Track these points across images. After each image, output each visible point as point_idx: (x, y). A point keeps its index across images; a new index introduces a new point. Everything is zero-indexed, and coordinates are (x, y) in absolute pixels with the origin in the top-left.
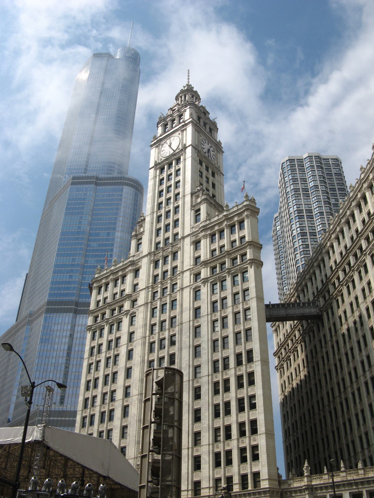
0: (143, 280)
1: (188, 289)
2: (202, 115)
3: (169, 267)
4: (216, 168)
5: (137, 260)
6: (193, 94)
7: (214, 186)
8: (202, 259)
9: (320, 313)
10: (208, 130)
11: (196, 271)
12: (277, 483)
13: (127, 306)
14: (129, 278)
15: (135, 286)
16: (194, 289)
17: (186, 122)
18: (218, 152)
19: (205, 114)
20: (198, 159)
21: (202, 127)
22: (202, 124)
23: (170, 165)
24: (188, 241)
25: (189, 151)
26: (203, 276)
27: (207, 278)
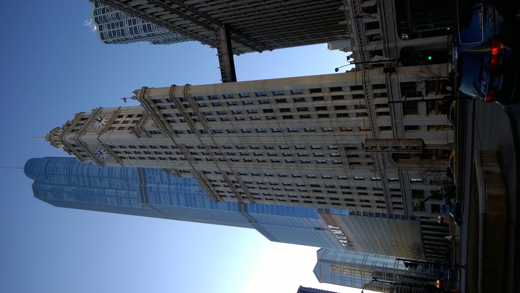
1: (214, 138)
2: (71, 128)
3: (199, 151)
4: (115, 114)
6: (52, 135)
7: (130, 116)
8: (189, 129)
9: (224, 26)
10: (83, 122)
12: (358, 72)
13: (232, 178)
14: (211, 177)
18: (101, 112)
19: (69, 125)
20: (109, 131)
21: (82, 127)
22: (78, 128)
23: (117, 152)
24: (176, 139)
25: (104, 137)
26: (203, 129)
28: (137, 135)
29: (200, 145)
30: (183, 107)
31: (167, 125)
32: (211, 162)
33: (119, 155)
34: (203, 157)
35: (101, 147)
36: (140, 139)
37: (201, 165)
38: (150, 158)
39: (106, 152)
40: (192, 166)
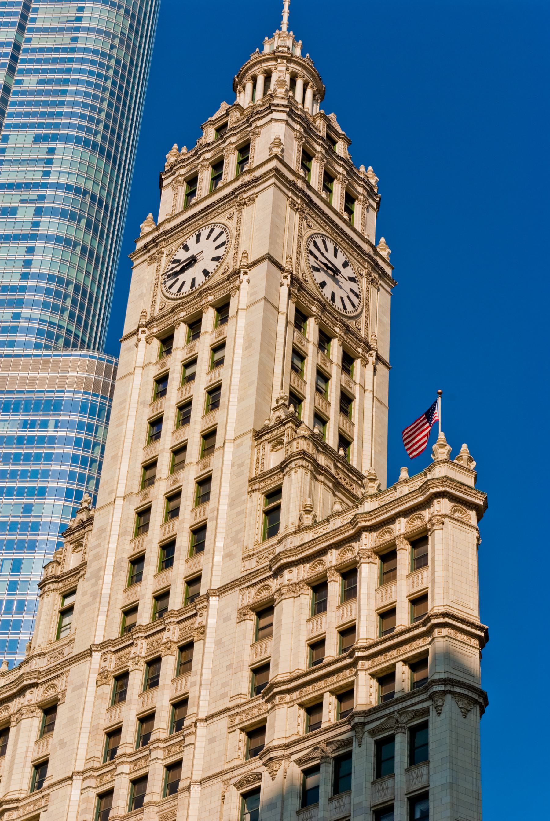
0: (77, 741)
1: (217, 786)
3: (162, 700)
5: (49, 672)
8: (274, 675)
11: (250, 718)
15: (41, 767)
16: (239, 785)
17: (257, 174)
20: (292, 307)
23: (194, 326)
27: (287, 746)
28: (267, 430)
29: (191, 709)
30: (382, 663)
31: (304, 572)
32: (99, 751)
33: (181, 333)
34: (128, 716)
35: (229, 264)
36: (248, 440)
37: (90, 698)
38: (150, 466)
39: (200, 279)
40: (89, 653)
